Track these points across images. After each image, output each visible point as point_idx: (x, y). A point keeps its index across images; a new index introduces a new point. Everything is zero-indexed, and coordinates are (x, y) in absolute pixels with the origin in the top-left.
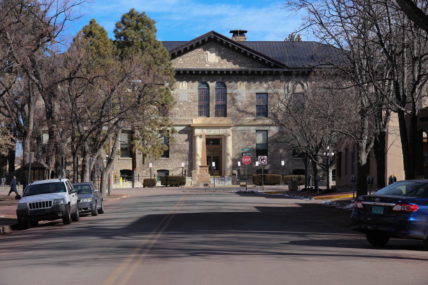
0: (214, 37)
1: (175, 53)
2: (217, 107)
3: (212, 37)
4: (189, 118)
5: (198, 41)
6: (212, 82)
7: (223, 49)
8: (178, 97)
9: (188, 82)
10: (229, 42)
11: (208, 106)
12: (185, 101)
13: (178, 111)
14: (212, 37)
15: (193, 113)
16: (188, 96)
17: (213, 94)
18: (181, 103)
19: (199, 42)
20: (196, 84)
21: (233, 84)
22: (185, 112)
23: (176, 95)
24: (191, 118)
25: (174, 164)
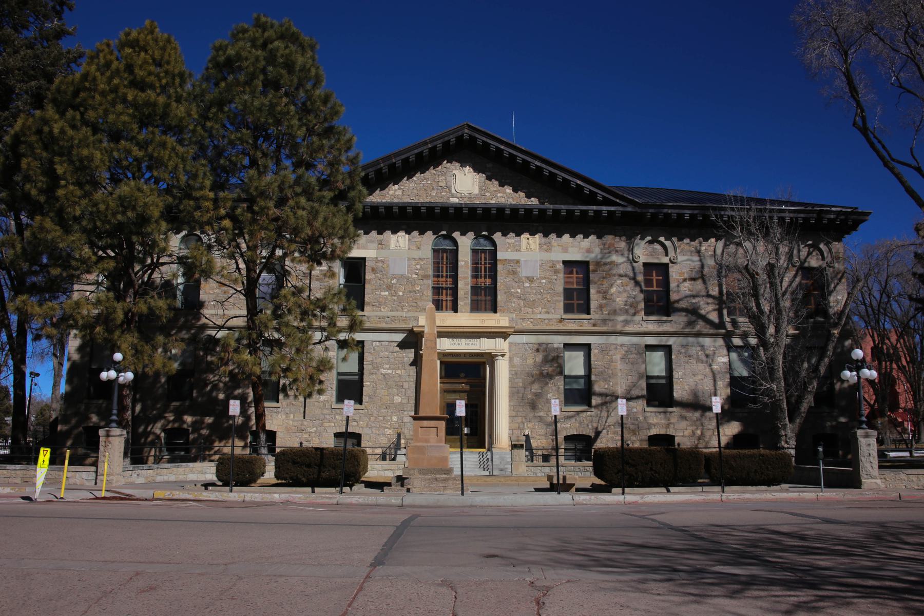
0: (470, 136)
1: (381, 169)
2: (475, 290)
3: (466, 137)
4: (410, 314)
5: (435, 143)
6: (463, 233)
7: (489, 165)
9: (409, 234)
10: (502, 147)
11: (455, 291)
12: (403, 277)
13: (385, 297)
14: (466, 137)
15: (420, 304)
16: (409, 266)
17: (466, 262)
18: (394, 281)
19: (435, 147)
20: (429, 236)
21: (511, 238)
22: (401, 300)
23: (383, 262)
24: (416, 314)
25: (372, 418)
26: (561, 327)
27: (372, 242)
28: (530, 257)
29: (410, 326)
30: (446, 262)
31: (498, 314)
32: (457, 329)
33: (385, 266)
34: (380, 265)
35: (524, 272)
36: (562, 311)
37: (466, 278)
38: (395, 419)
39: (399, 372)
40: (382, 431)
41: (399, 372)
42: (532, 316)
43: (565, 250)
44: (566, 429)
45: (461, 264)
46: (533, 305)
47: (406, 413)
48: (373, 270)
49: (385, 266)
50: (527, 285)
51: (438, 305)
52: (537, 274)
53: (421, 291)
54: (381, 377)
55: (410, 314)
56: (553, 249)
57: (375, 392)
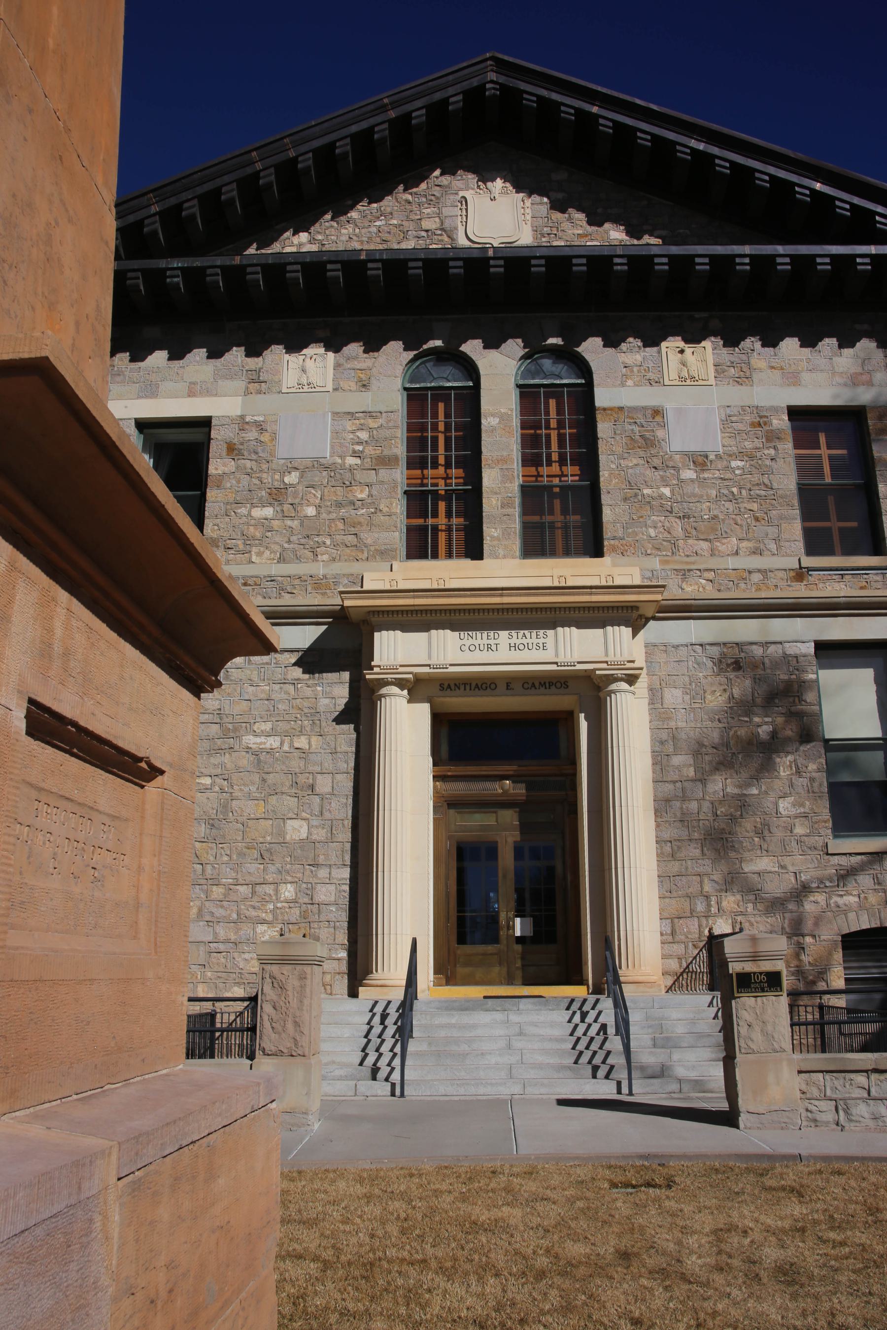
0: (503, 87)
1: (256, 175)
2: (533, 497)
3: (491, 90)
4: (338, 568)
6: (492, 343)
8: (273, 438)
9: (337, 350)
11: (470, 501)
13: (265, 524)
15: (368, 538)
16: (336, 433)
17: (503, 417)
18: (292, 478)
19: (408, 116)
20: (395, 357)
21: (632, 352)
23: (260, 427)
26: (800, 591)
27: (231, 377)
28: (691, 402)
29: (333, 601)
30: (444, 426)
31: (607, 560)
32: (480, 619)
33: (265, 437)
34: (252, 434)
35: (679, 438)
36: (800, 545)
37: (503, 460)
38: (288, 891)
39: (301, 742)
40: (246, 930)
41: (301, 742)
42: (713, 563)
43: (793, 379)
44: (843, 911)
45: (488, 422)
46: (712, 531)
47: (323, 873)
48: (232, 449)
49: (265, 437)
50: (689, 474)
51: (420, 546)
52: (714, 442)
53: (372, 503)
54: (245, 760)
55: (338, 568)
56: (755, 376)
57: (225, 807)
